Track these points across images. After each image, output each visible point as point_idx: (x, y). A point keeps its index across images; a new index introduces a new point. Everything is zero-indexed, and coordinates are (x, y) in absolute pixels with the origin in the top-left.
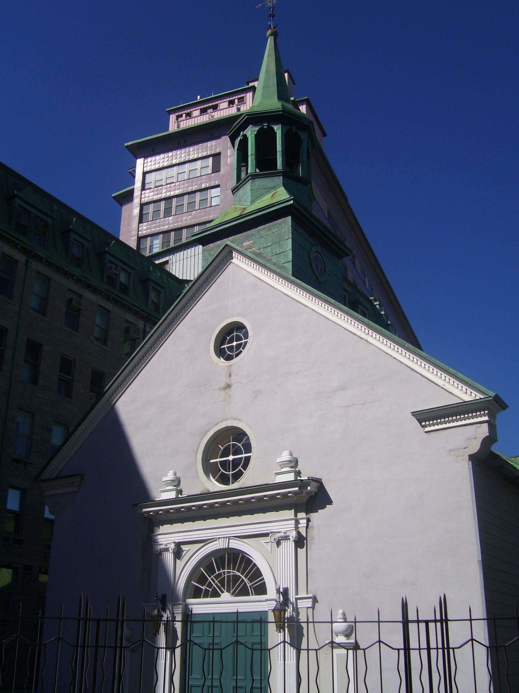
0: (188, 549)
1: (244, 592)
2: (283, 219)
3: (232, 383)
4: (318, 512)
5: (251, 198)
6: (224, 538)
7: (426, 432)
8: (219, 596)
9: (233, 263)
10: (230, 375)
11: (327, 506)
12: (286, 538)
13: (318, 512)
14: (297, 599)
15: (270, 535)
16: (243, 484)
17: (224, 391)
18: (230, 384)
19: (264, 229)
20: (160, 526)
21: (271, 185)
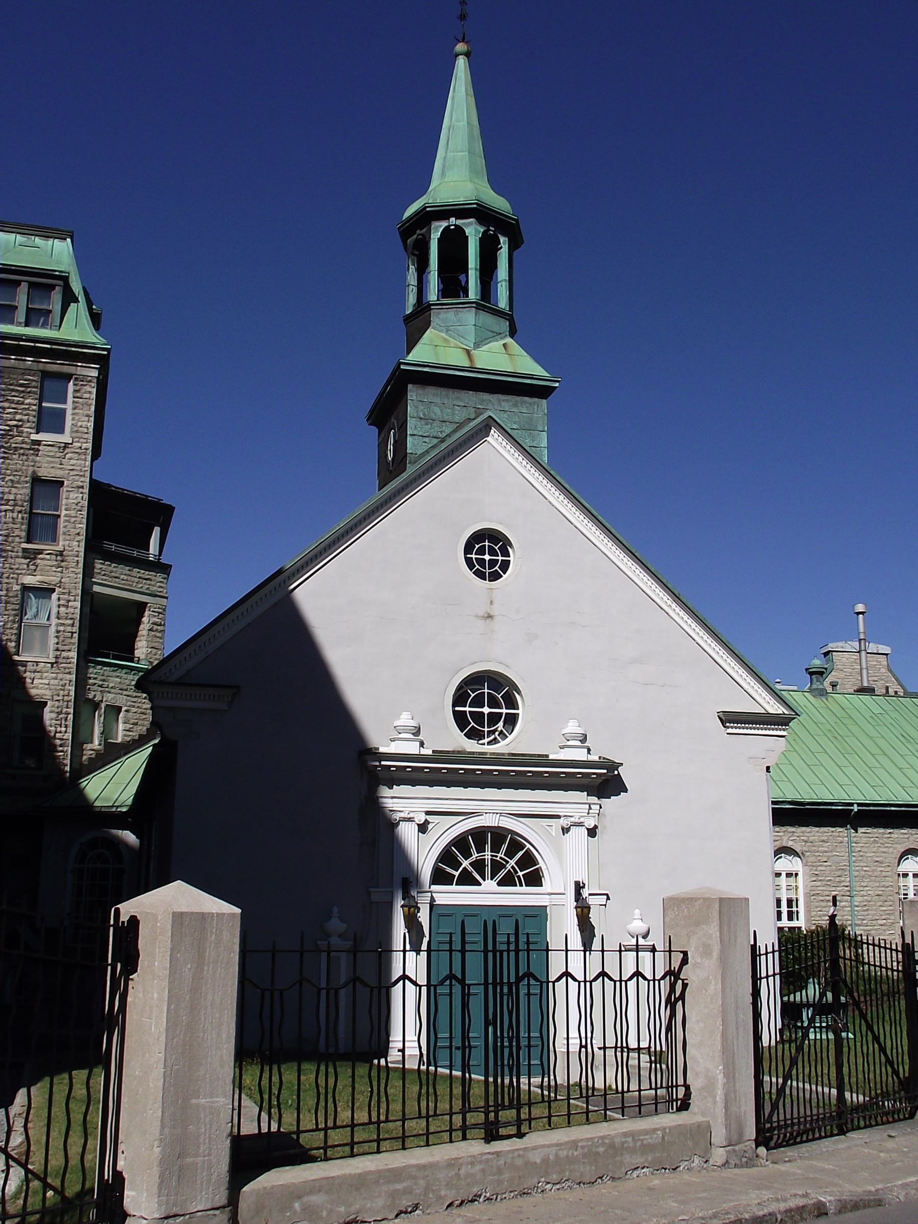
0: (437, 822)
1: (508, 881)
2: (536, 400)
3: (496, 614)
4: (610, 798)
5: (475, 339)
6: (494, 813)
7: (728, 734)
8: (480, 884)
9: (488, 442)
10: (491, 603)
11: (622, 793)
12: (580, 824)
13: (610, 798)
14: (590, 895)
15: (562, 818)
16: (513, 749)
17: (484, 621)
18: (492, 614)
19: (507, 401)
20: (394, 786)
21: (496, 329)
